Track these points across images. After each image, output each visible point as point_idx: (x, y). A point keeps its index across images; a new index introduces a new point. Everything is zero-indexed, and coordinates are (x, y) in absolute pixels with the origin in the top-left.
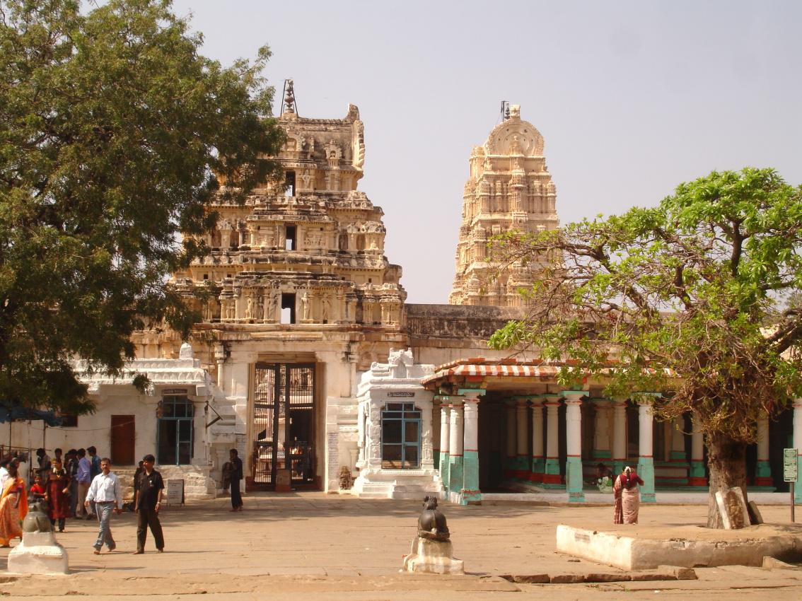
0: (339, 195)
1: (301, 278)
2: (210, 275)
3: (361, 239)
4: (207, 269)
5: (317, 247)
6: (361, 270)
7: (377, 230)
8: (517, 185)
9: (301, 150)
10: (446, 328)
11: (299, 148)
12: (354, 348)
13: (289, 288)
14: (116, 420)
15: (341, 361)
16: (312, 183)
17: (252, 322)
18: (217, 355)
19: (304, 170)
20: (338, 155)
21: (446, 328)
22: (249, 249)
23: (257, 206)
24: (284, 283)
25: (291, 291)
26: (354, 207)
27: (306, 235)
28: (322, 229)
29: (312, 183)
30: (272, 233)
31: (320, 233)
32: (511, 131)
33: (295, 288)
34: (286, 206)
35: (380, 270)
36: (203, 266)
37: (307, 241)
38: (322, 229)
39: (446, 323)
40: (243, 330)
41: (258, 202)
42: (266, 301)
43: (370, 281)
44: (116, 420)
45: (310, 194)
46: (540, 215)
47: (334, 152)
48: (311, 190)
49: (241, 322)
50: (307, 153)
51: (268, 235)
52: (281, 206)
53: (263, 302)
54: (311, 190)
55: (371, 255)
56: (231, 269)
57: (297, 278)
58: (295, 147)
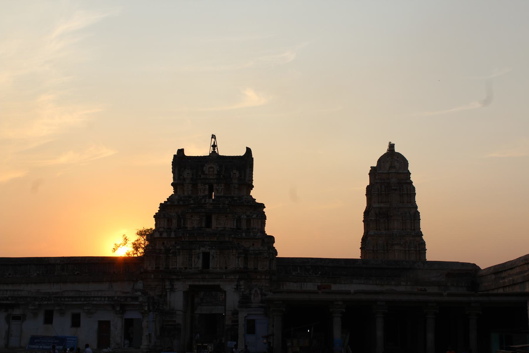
2: (165, 242)
3: (248, 221)
7: (257, 216)
8: (393, 188)
10: (299, 271)
11: (216, 172)
12: (242, 283)
14: (101, 323)
15: (234, 290)
17: (186, 268)
18: (167, 287)
21: (299, 271)
23: (192, 204)
25: (207, 250)
28: (226, 216)
38: (226, 216)
39: (299, 268)
43: (253, 245)
44: (101, 323)
47: (235, 174)
54: (222, 194)
55: (254, 230)
58: (213, 171)
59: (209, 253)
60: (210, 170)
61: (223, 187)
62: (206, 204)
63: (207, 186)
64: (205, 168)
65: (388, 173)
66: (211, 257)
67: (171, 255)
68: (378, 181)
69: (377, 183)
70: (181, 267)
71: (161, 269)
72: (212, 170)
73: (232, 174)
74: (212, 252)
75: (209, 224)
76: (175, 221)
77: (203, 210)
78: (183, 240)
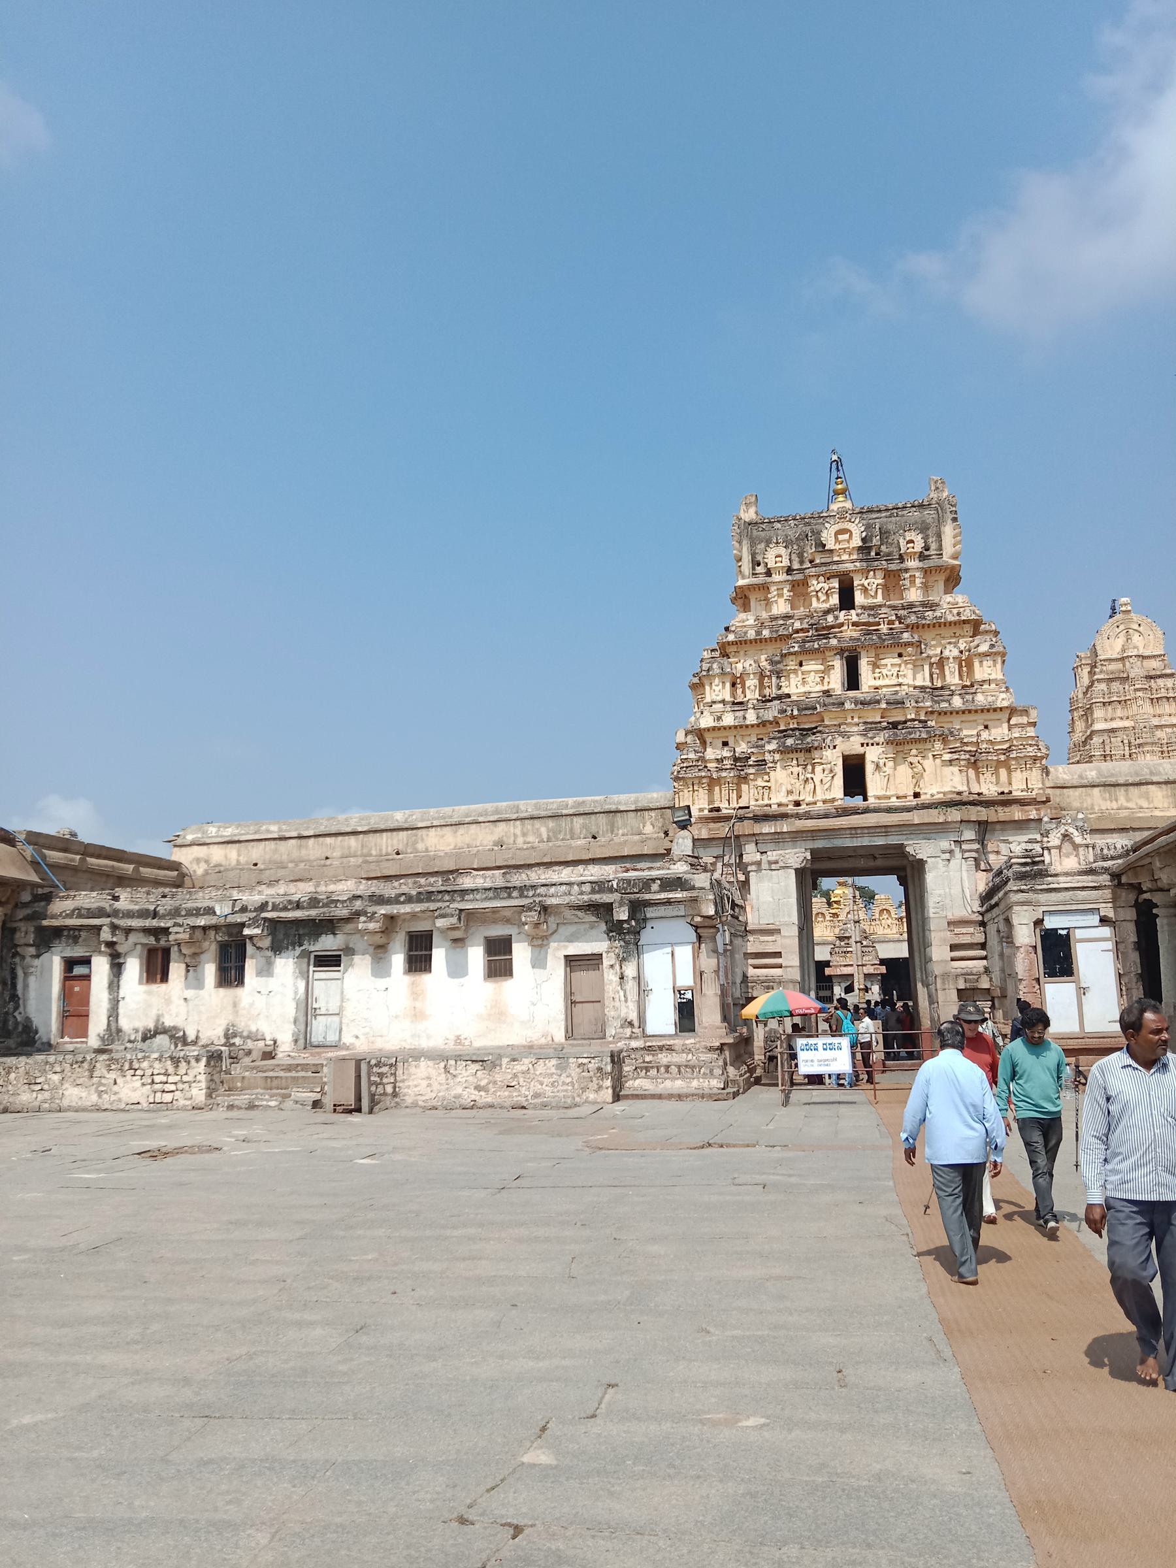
0: (924, 604)
1: (871, 729)
3: (966, 664)
4: (724, 733)
5: (894, 681)
6: (970, 711)
9: (860, 544)
11: (857, 542)
13: (854, 745)
16: (880, 591)
19: (865, 573)
20: (919, 546)
22: (788, 696)
23: (797, 631)
24: (846, 735)
26: (950, 618)
27: (875, 665)
29: (880, 591)
30: (822, 667)
31: (897, 661)
32: (1122, 627)
33: (862, 745)
34: (842, 625)
35: (1001, 709)
36: (719, 729)
37: (877, 675)
38: (900, 655)
40: (784, 816)
41: (797, 625)
42: (818, 769)
45: (880, 606)
46: (1167, 718)
47: (912, 541)
48: (880, 599)
49: (779, 805)
50: (870, 548)
51: (816, 672)
52: (833, 627)
53: (813, 772)
54: (880, 599)
55: (986, 686)
56: (761, 730)
57: (865, 730)
59: (861, 758)
60: (841, 537)
61: (880, 581)
62: (842, 625)
63: (835, 584)
64: (824, 534)
65: (1122, 659)
66: (869, 768)
67: (752, 770)
68: (1101, 676)
69: (1099, 680)
70: (784, 801)
71: (724, 811)
72: (846, 536)
73: (902, 543)
74: (873, 755)
75: (853, 681)
76: (752, 682)
77: (834, 642)
78: (782, 728)
